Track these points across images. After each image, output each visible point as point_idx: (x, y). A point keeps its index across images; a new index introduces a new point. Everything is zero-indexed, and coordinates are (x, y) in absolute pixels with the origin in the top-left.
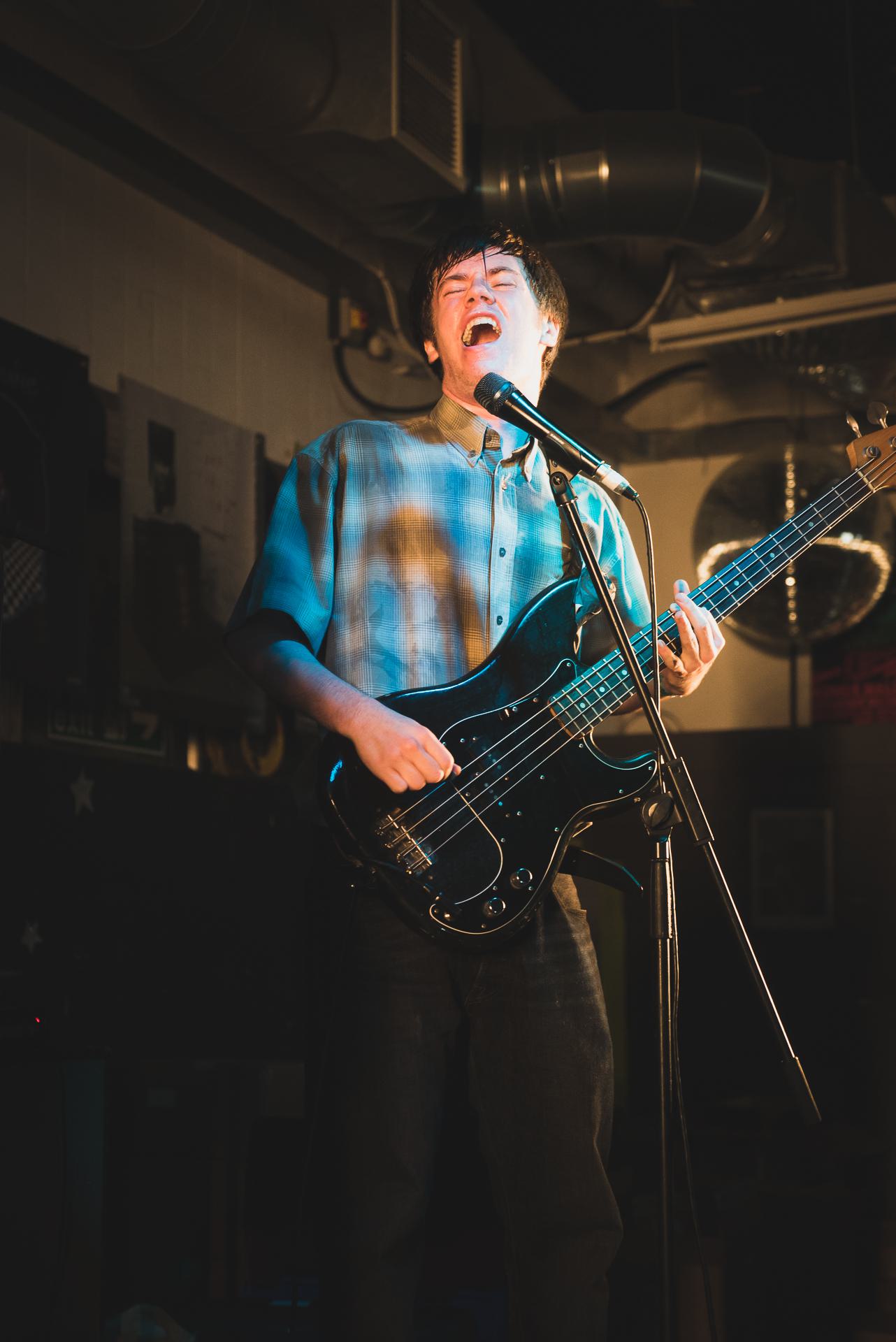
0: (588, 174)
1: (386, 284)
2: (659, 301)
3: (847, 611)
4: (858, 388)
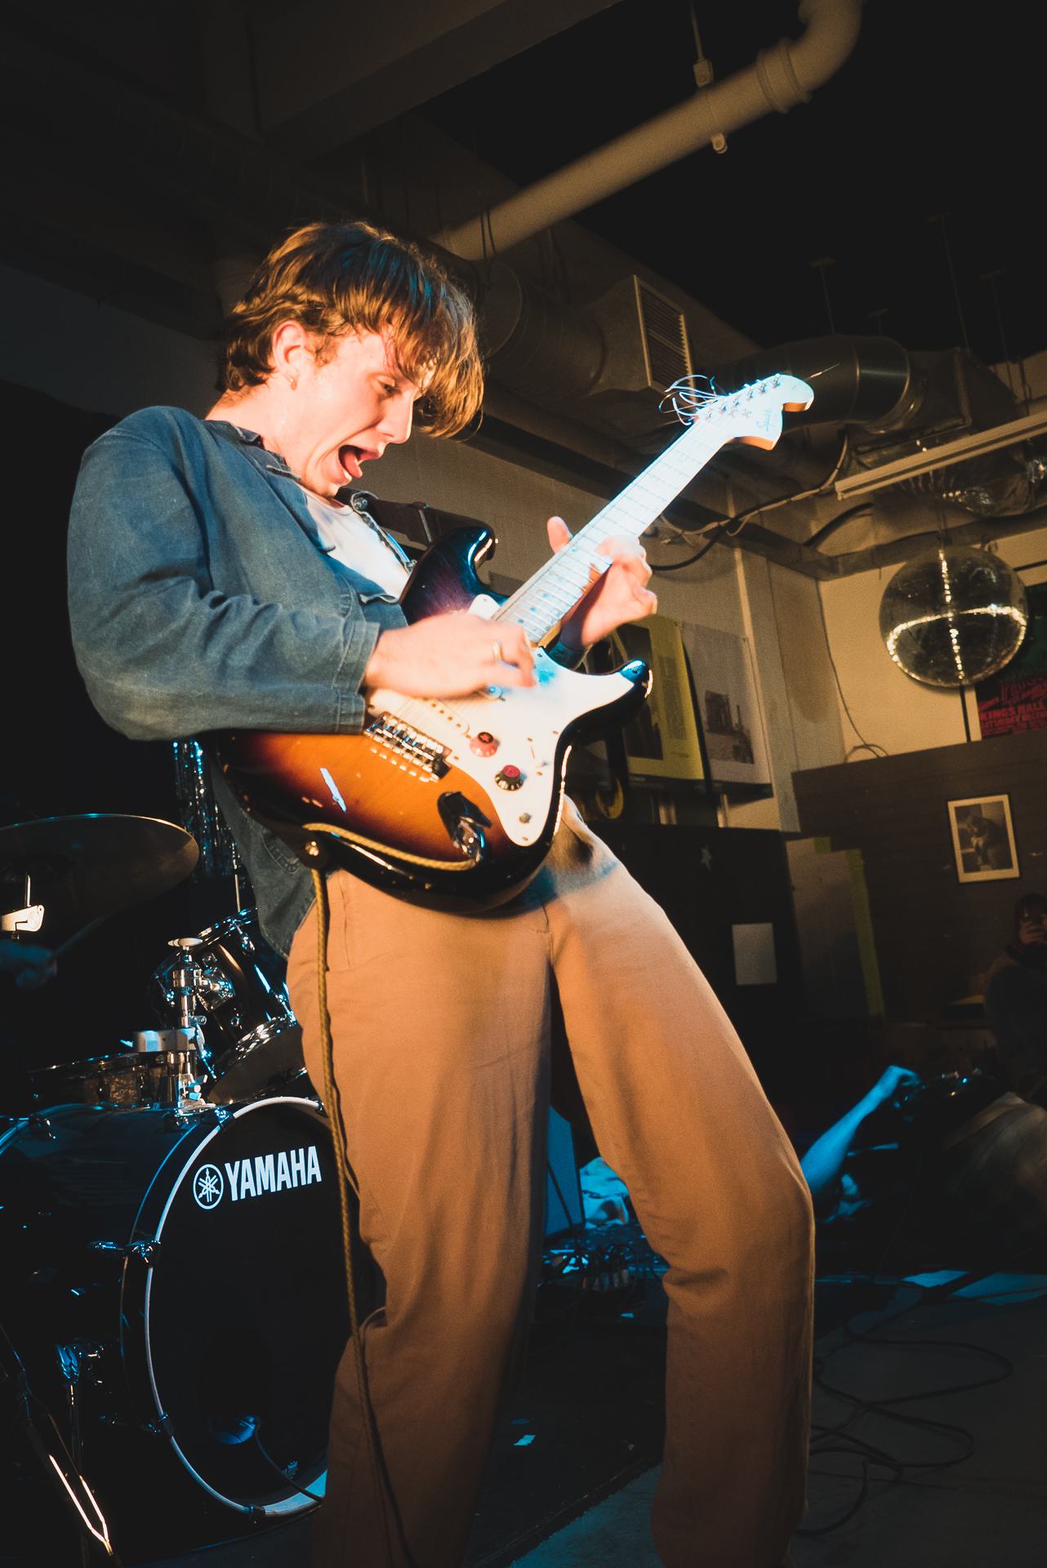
2: (839, 465)
3: (998, 657)
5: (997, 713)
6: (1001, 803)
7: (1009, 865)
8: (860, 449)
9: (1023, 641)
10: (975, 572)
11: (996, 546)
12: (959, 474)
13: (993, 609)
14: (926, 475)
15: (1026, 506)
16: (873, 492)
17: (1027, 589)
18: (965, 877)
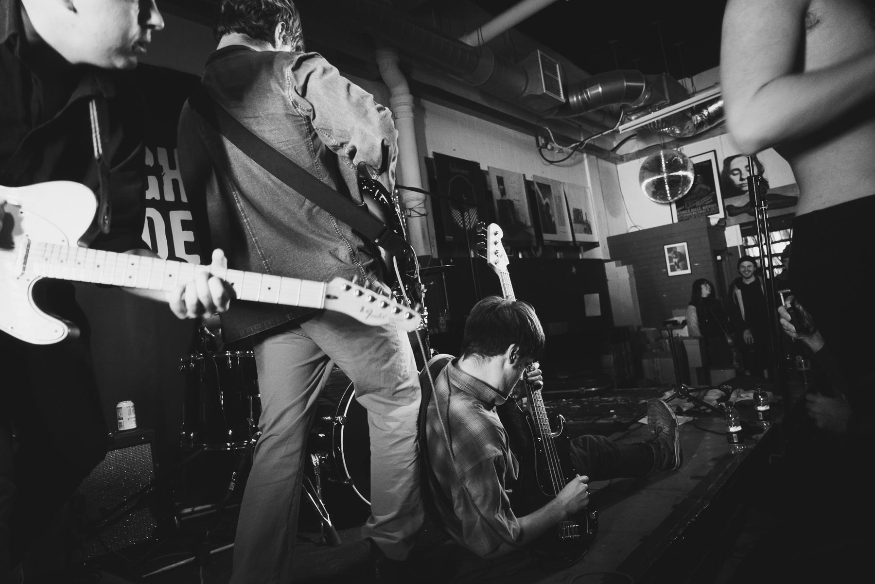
0: (596, 91)
1: (549, 131)
2: (620, 120)
3: (683, 191)
4: (678, 132)
5: (684, 212)
6: (684, 246)
7: (687, 268)
8: (628, 114)
9: (693, 185)
10: (674, 159)
11: (683, 149)
12: (667, 121)
13: (681, 173)
14: (654, 122)
15: (693, 133)
16: (634, 129)
17: (694, 165)
18: (671, 274)
